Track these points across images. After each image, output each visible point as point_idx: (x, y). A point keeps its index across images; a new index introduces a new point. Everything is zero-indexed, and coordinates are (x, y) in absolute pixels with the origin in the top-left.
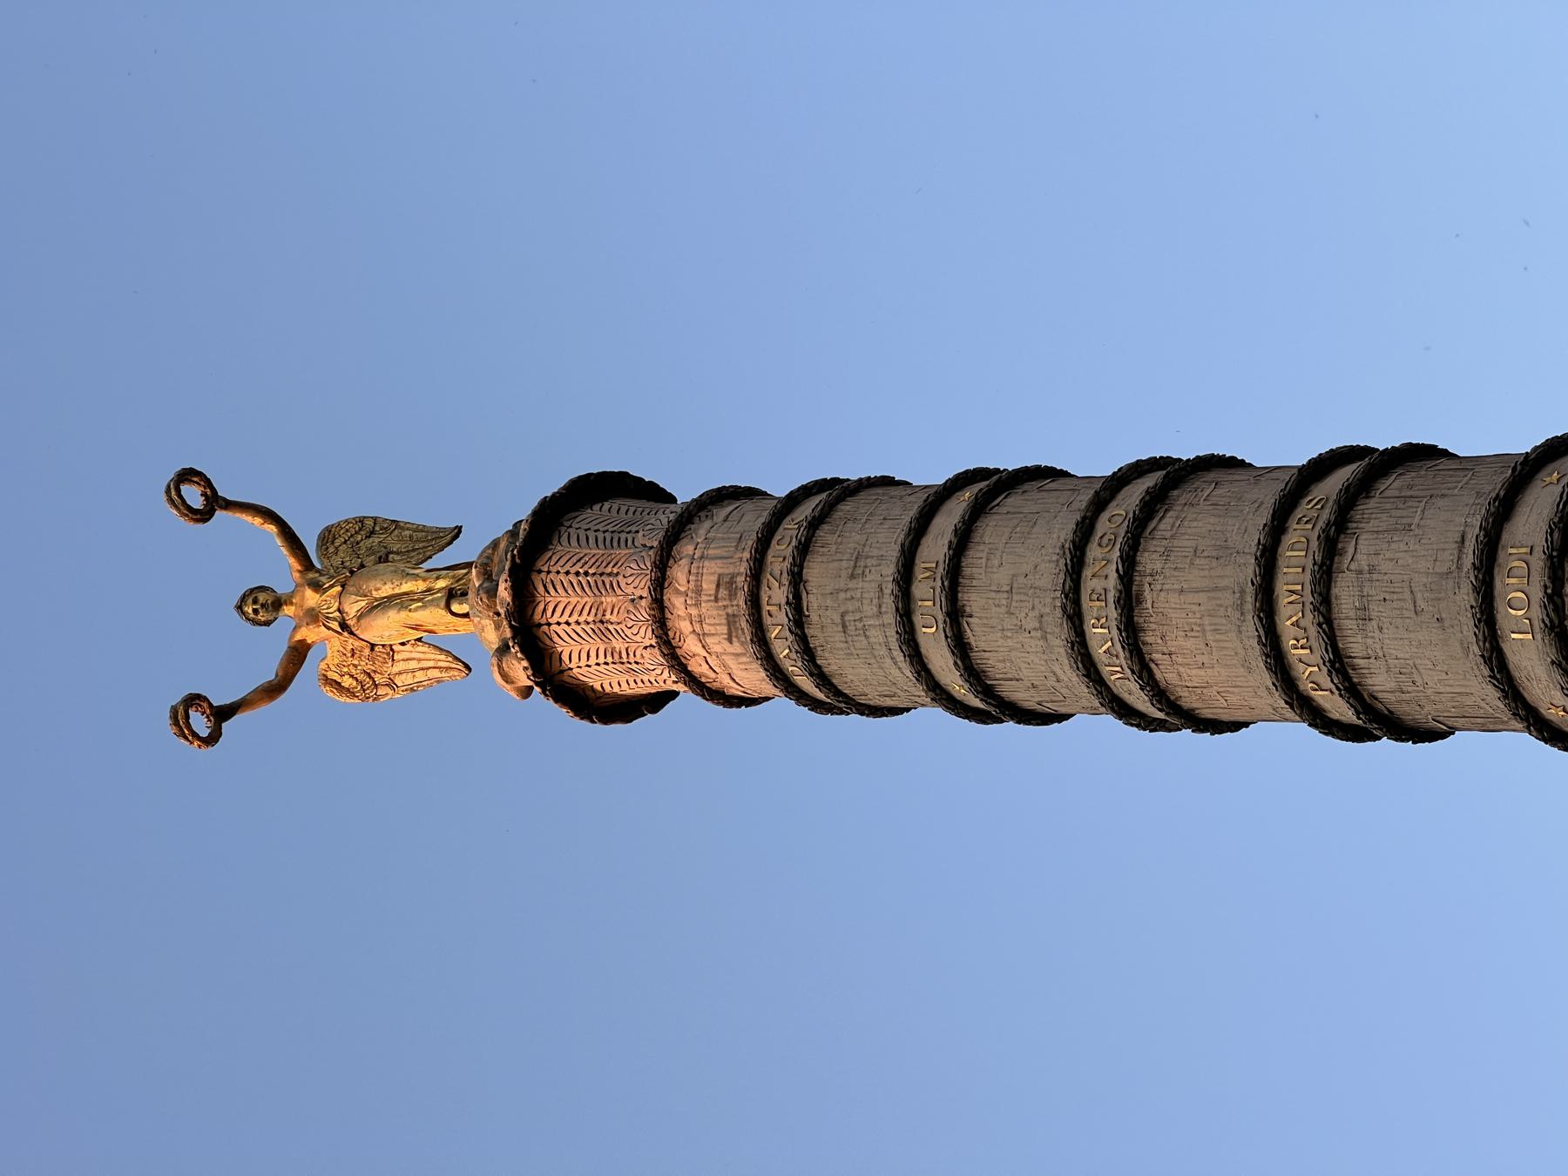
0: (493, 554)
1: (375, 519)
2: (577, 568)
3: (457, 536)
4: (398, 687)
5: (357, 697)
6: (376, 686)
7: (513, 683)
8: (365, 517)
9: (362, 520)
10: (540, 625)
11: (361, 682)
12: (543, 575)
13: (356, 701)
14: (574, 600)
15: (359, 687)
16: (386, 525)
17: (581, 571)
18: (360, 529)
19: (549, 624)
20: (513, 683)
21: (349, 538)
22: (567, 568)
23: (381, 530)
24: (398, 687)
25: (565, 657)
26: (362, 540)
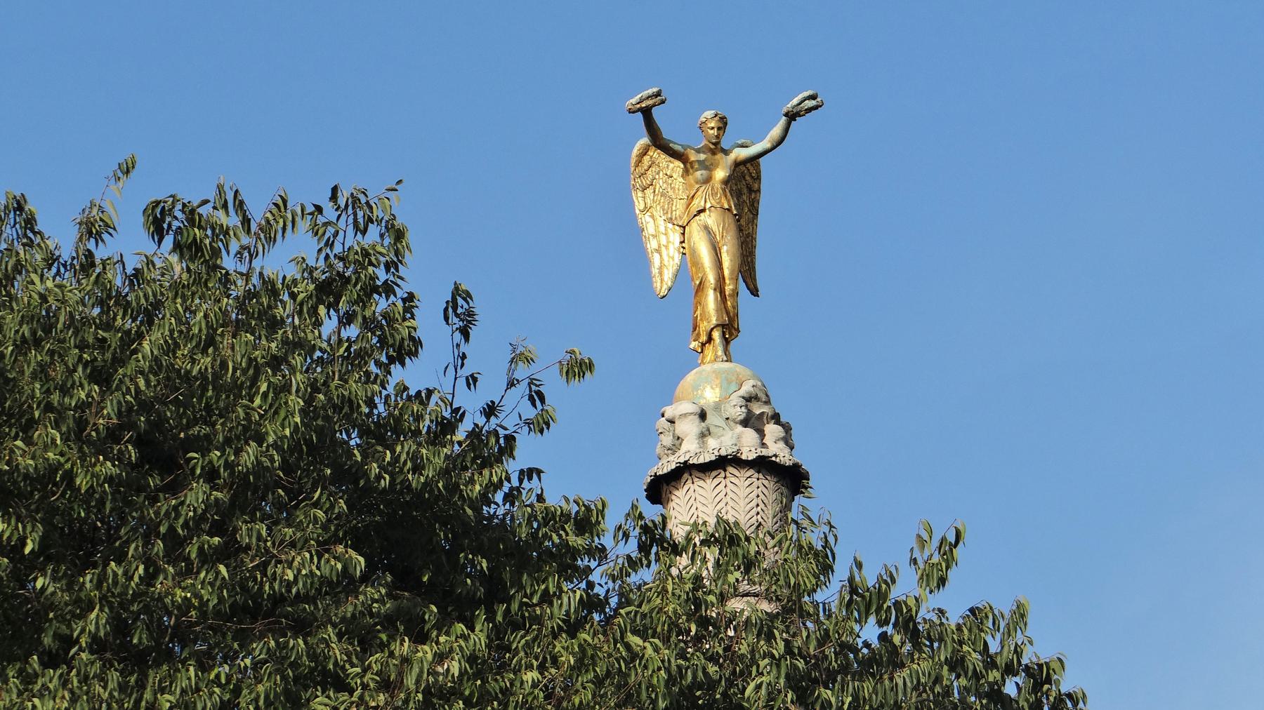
1: (759, 190)
2: (762, 505)
3: (752, 294)
6: (644, 189)
7: (679, 418)
9: (758, 178)
10: (725, 471)
12: (756, 475)
13: (633, 169)
14: (742, 503)
17: (759, 508)
18: (753, 177)
19: (725, 478)
20: (679, 418)
22: (762, 496)
25: (701, 483)
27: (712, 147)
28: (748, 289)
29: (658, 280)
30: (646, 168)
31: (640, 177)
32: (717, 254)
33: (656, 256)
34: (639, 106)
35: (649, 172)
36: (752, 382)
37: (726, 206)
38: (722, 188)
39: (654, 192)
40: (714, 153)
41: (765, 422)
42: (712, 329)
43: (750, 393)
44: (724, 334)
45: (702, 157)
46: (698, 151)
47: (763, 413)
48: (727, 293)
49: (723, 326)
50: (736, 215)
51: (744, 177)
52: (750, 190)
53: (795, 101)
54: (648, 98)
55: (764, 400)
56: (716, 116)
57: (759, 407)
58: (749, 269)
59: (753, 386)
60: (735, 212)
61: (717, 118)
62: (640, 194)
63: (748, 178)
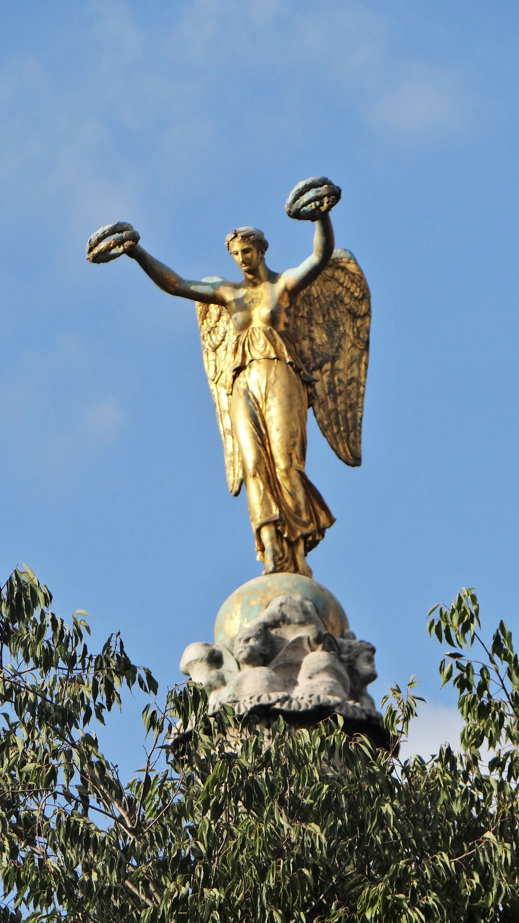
0: (295, 623)
1: (368, 314)
4: (216, 383)
5: (203, 324)
6: (215, 350)
8: (369, 298)
9: (366, 296)
11: (216, 327)
13: (200, 323)
15: (212, 325)
16: (361, 336)
18: (356, 298)
21: (346, 287)
23: (358, 329)
24: (216, 383)
26: (346, 305)
27: (250, 277)
28: (340, 458)
29: (232, 472)
30: (215, 318)
31: (209, 332)
32: (256, 425)
33: (229, 438)
34: (92, 253)
35: (219, 324)
36: (280, 599)
37: (273, 355)
38: (265, 333)
39: (226, 349)
40: (255, 285)
41: (308, 648)
42: (259, 531)
43: (273, 615)
44: (279, 534)
45: (242, 292)
46: (236, 287)
47: (299, 640)
48: (279, 477)
49: (275, 523)
50: (291, 364)
51: (342, 301)
52: (355, 316)
53: (290, 198)
54: (100, 240)
55: (297, 620)
56: (236, 236)
57: (294, 631)
58: (347, 430)
59: (281, 605)
60: (288, 360)
61: (239, 238)
62: (212, 356)
63: (347, 300)
